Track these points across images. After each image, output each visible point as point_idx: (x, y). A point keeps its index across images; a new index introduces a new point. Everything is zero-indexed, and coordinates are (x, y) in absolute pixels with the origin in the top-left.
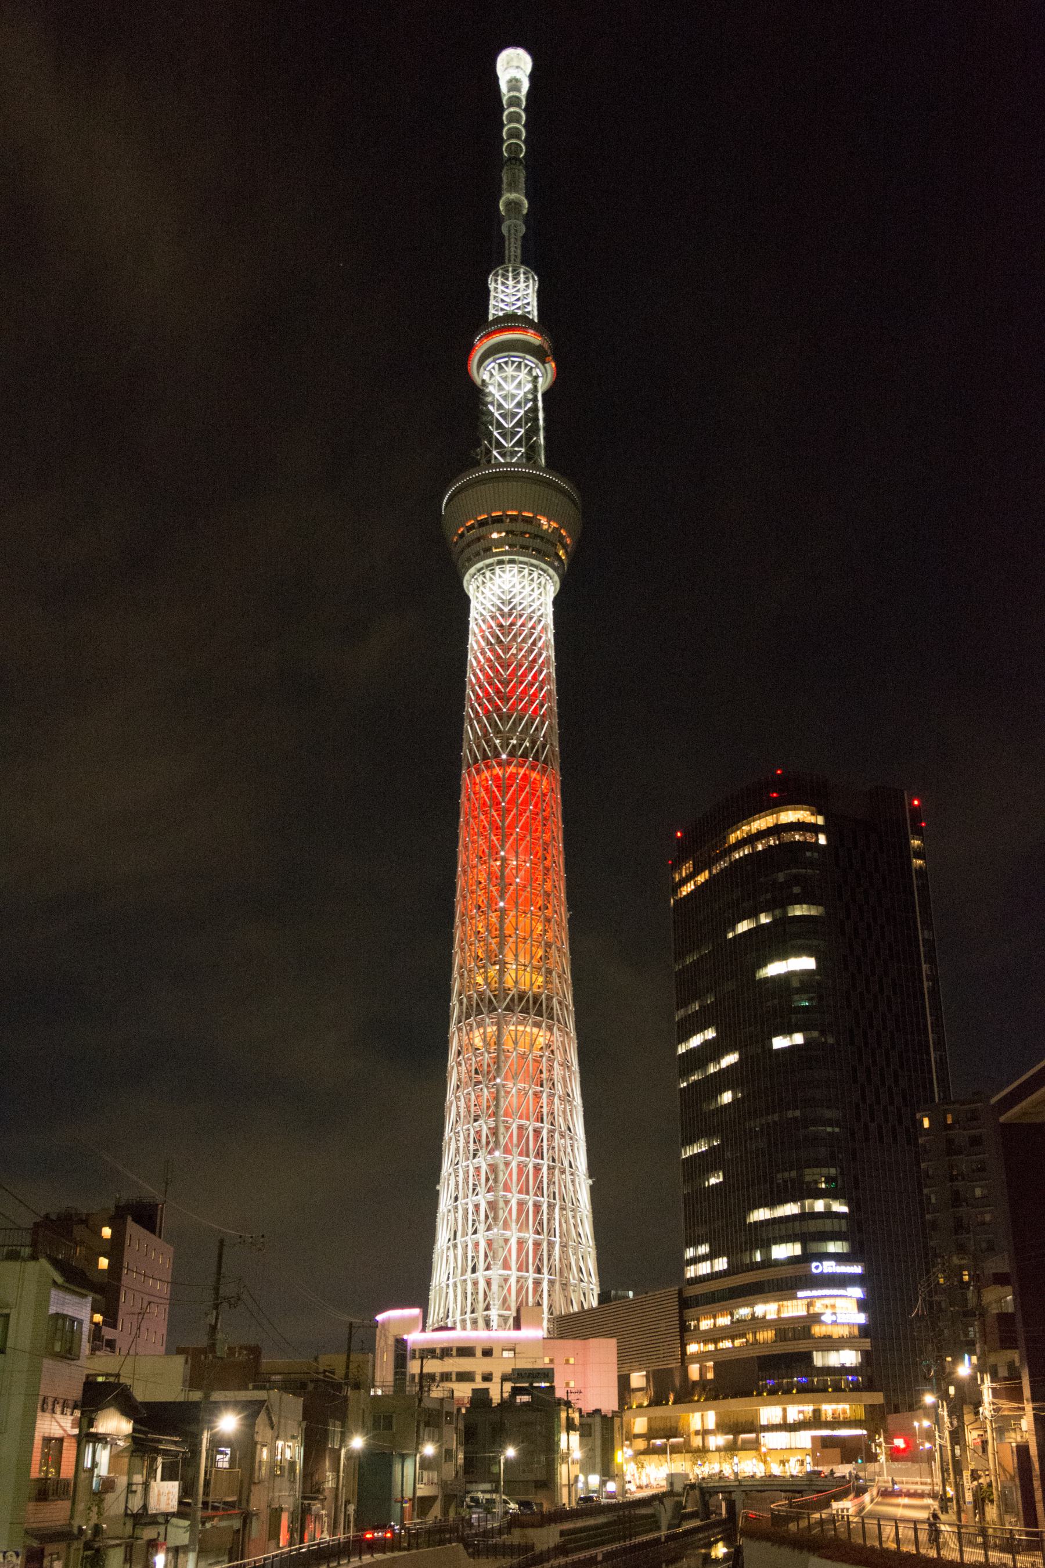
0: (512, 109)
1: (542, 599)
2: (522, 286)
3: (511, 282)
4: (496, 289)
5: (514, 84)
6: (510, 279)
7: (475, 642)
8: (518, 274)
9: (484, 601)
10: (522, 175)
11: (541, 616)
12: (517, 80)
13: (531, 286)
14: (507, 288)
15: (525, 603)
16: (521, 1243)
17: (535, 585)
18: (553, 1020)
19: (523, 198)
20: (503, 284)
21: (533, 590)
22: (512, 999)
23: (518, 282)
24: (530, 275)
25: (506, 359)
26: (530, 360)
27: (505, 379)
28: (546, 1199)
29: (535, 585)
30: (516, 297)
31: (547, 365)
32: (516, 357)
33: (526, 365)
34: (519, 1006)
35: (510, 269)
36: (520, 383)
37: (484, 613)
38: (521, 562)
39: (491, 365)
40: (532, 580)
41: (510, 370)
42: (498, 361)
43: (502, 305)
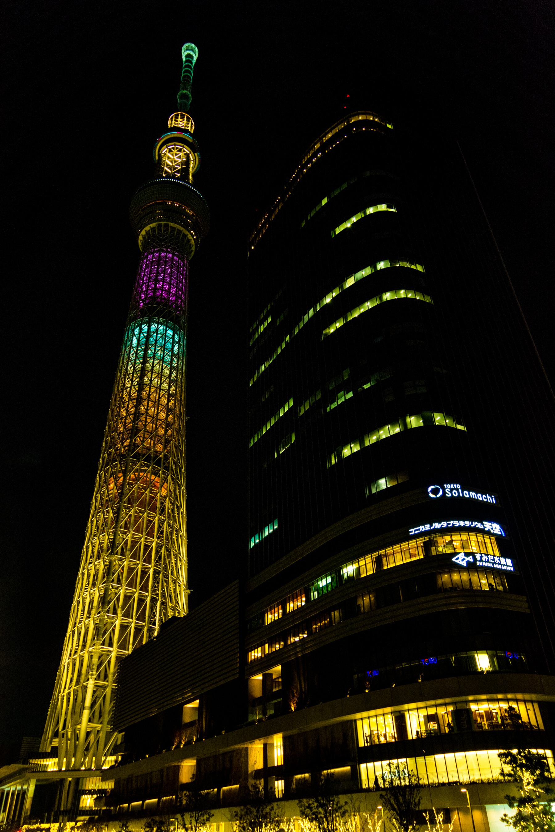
6: (179, 118)
10: (189, 87)
16: (124, 628)
18: (169, 472)
20: (175, 120)
25: (174, 146)
26: (187, 150)
27: (172, 155)
28: (150, 594)
31: (196, 154)
32: (179, 146)
33: (184, 151)
36: (180, 156)
39: (165, 150)
41: (175, 151)
42: (169, 148)
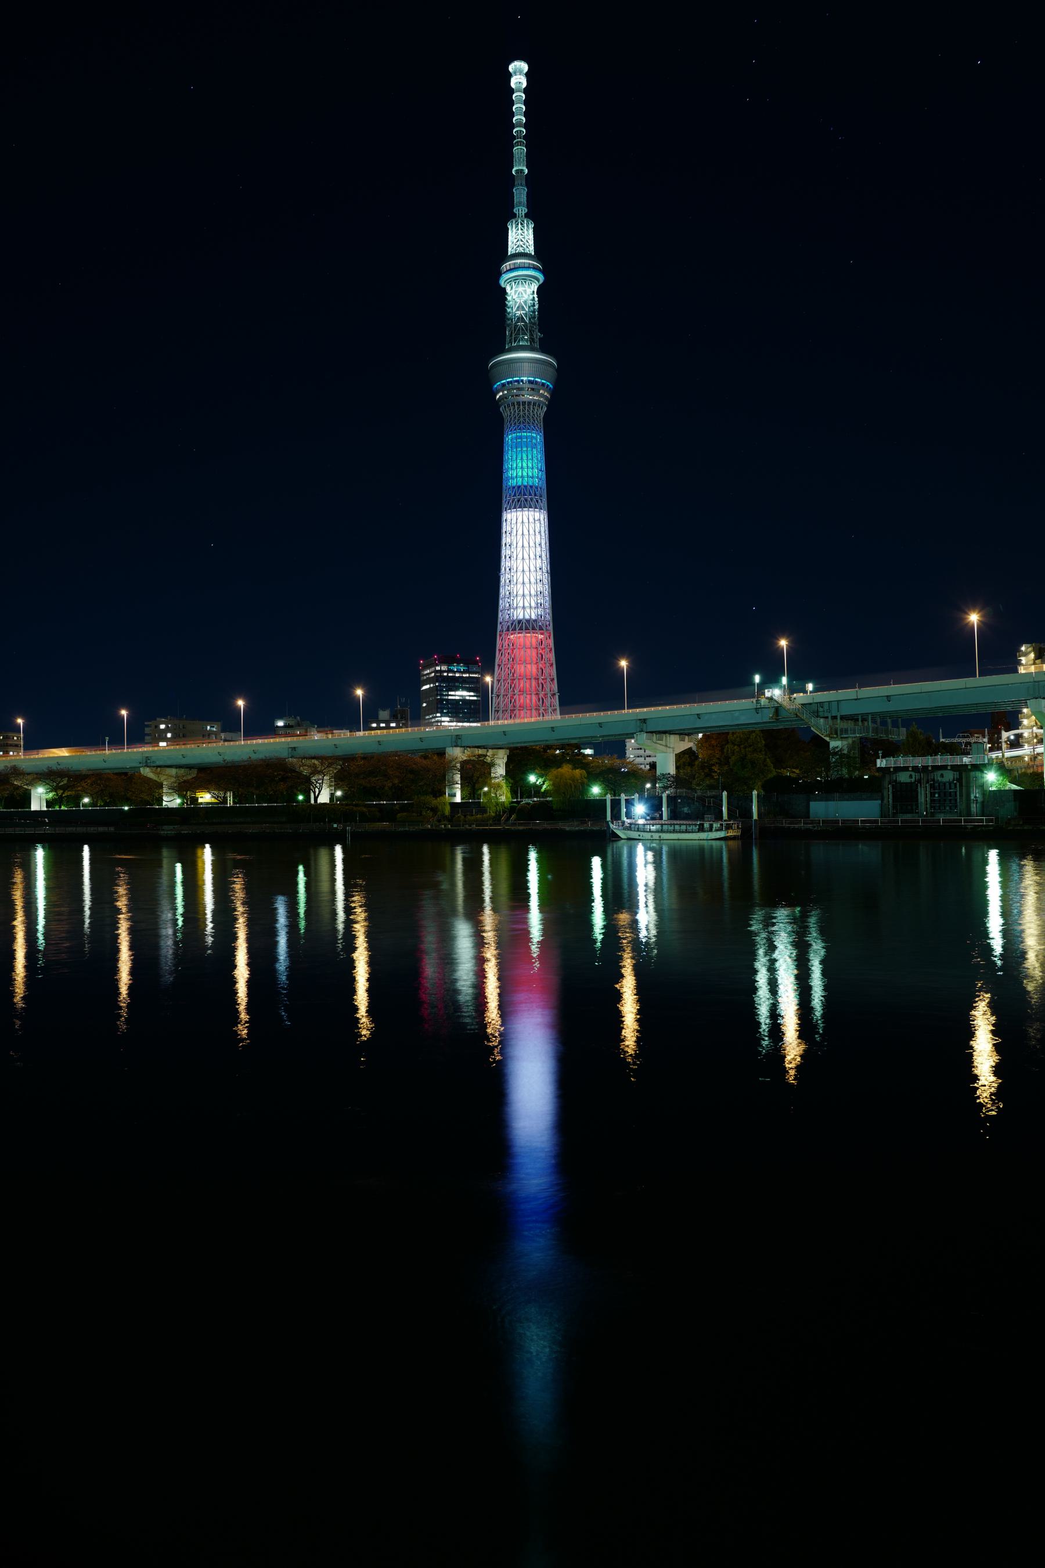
2: (520, 231)
8: (518, 224)
12: (520, 83)
24: (525, 222)
30: (517, 240)
35: (514, 222)
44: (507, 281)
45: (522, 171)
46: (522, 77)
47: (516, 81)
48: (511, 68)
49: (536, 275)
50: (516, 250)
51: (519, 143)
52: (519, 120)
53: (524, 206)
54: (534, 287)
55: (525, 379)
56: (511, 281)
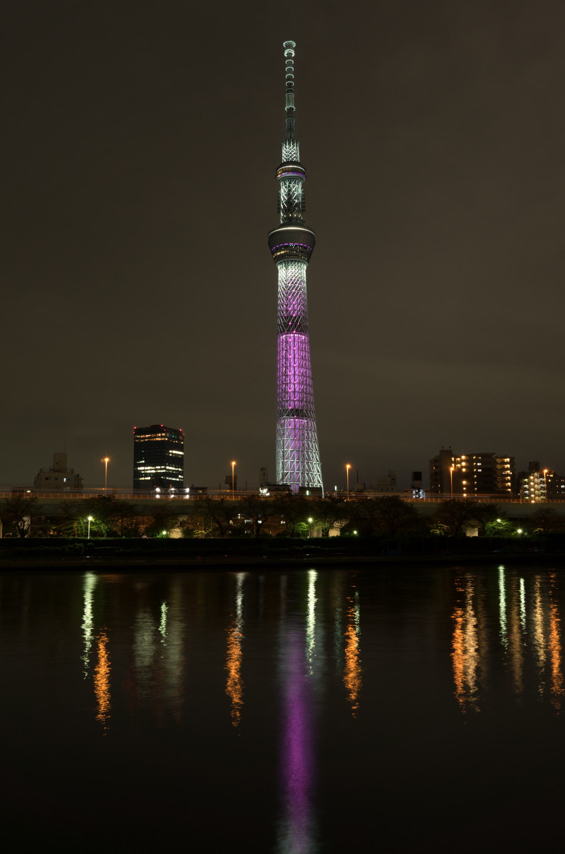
0: (289, 67)
1: (300, 271)
3: (287, 146)
4: (283, 148)
5: (289, 54)
6: (287, 145)
7: (279, 290)
8: (291, 143)
9: (281, 275)
11: (299, 278)
12: (290, 53)
13: (295, 145)
14: (286, 149)
15: (293, 275)
17: (296, 267)
19: (294, 107)
20: (285, 147)
21: (296, 270)
22: (289, 411)
23: (290, 146)
24: (295, 141)
27: (286, 187)
29: (296, 267)
34: (291, 414)
37: (281, 279)
38: (291, 261)
40: (296, 265)
43: (285, 156)
44: (284, 179)
45: (291, 109)
46: (292, 50)
47: (288, 52)
48: (284, 44)
49: (300, 176)
50: (289, 159)
51: (291, 91)
52: (289, 77)
53: (292, 131)
54: (300, 184)
55: (291, 244)
56: (286, 179)
